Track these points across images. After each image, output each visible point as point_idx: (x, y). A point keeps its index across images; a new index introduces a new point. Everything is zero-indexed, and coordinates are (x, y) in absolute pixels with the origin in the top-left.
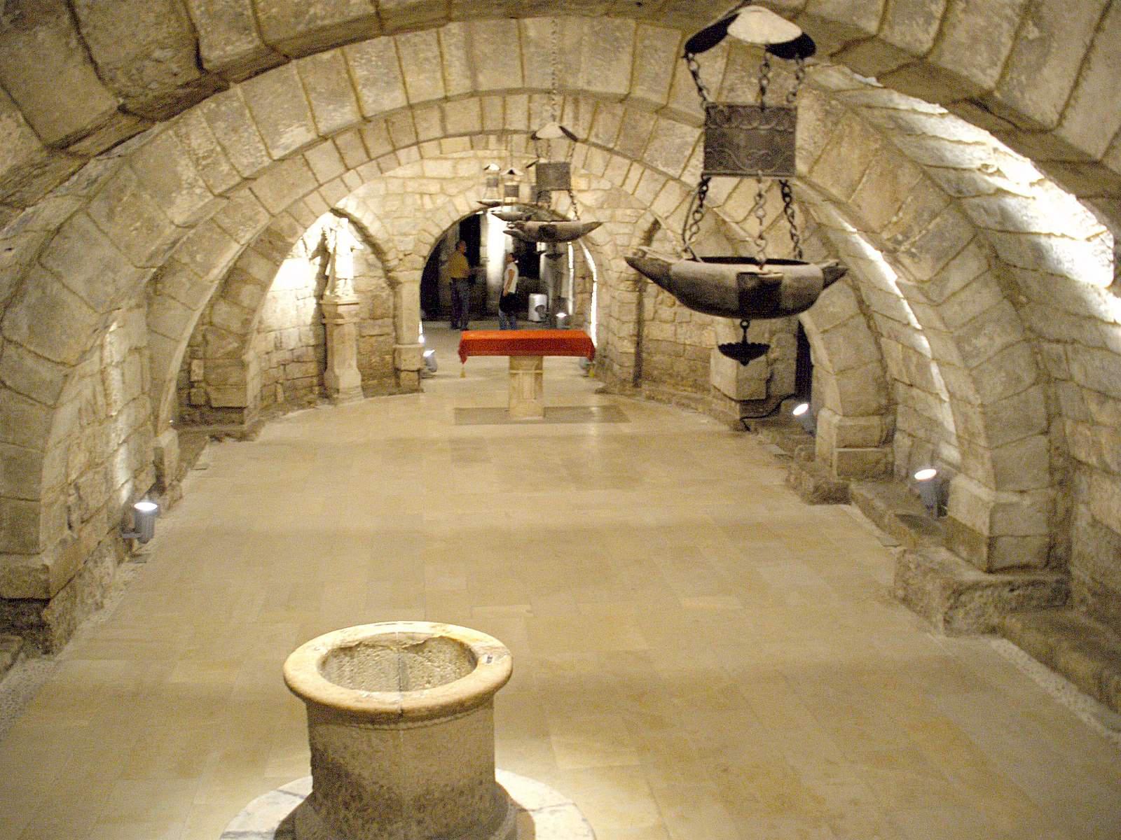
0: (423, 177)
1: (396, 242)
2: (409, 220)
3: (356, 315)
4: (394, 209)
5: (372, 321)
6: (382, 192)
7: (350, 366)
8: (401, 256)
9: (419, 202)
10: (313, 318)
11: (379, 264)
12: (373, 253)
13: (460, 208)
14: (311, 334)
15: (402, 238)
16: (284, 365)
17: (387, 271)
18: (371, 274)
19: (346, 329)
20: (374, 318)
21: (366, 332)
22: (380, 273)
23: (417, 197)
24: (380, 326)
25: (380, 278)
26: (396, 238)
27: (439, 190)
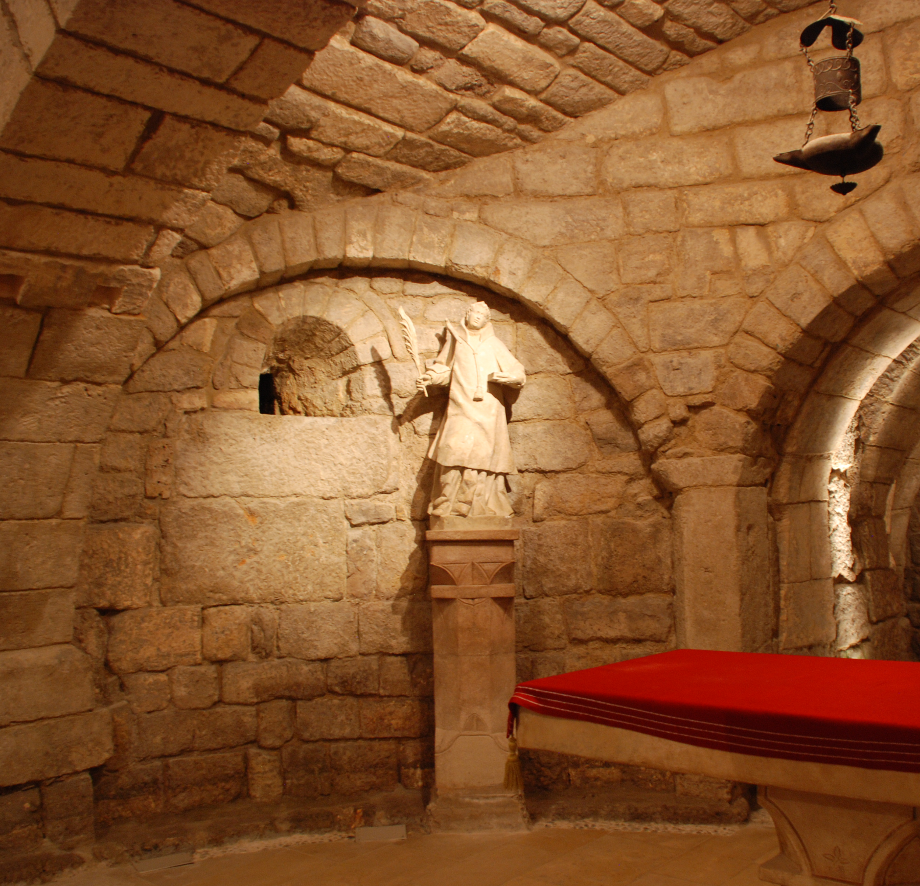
0: (735, 177)
1: (660, 372)
2: (697, 305)
3: (506, 572)
4: (652, 273)
5: (606, 600)
6: (614, 228)
7: (475, 723)
8: (679, 411)
9: (726, 250)
10: (404, 578)
11: (627, 438)
12: (608, 406)
13: (849, 256)
14: (396, 622)
15: (676, 358)
16: (293, 699)
17: (649, 455)
18: (607, 465)
19: (462, 614)
20: (613, 591)
21: (586, 629)
22: (631, 462)
23: (721, 236)
24: (631, 617)
25: (632, 479)
26: (657, 359)
27: (783, 211)
